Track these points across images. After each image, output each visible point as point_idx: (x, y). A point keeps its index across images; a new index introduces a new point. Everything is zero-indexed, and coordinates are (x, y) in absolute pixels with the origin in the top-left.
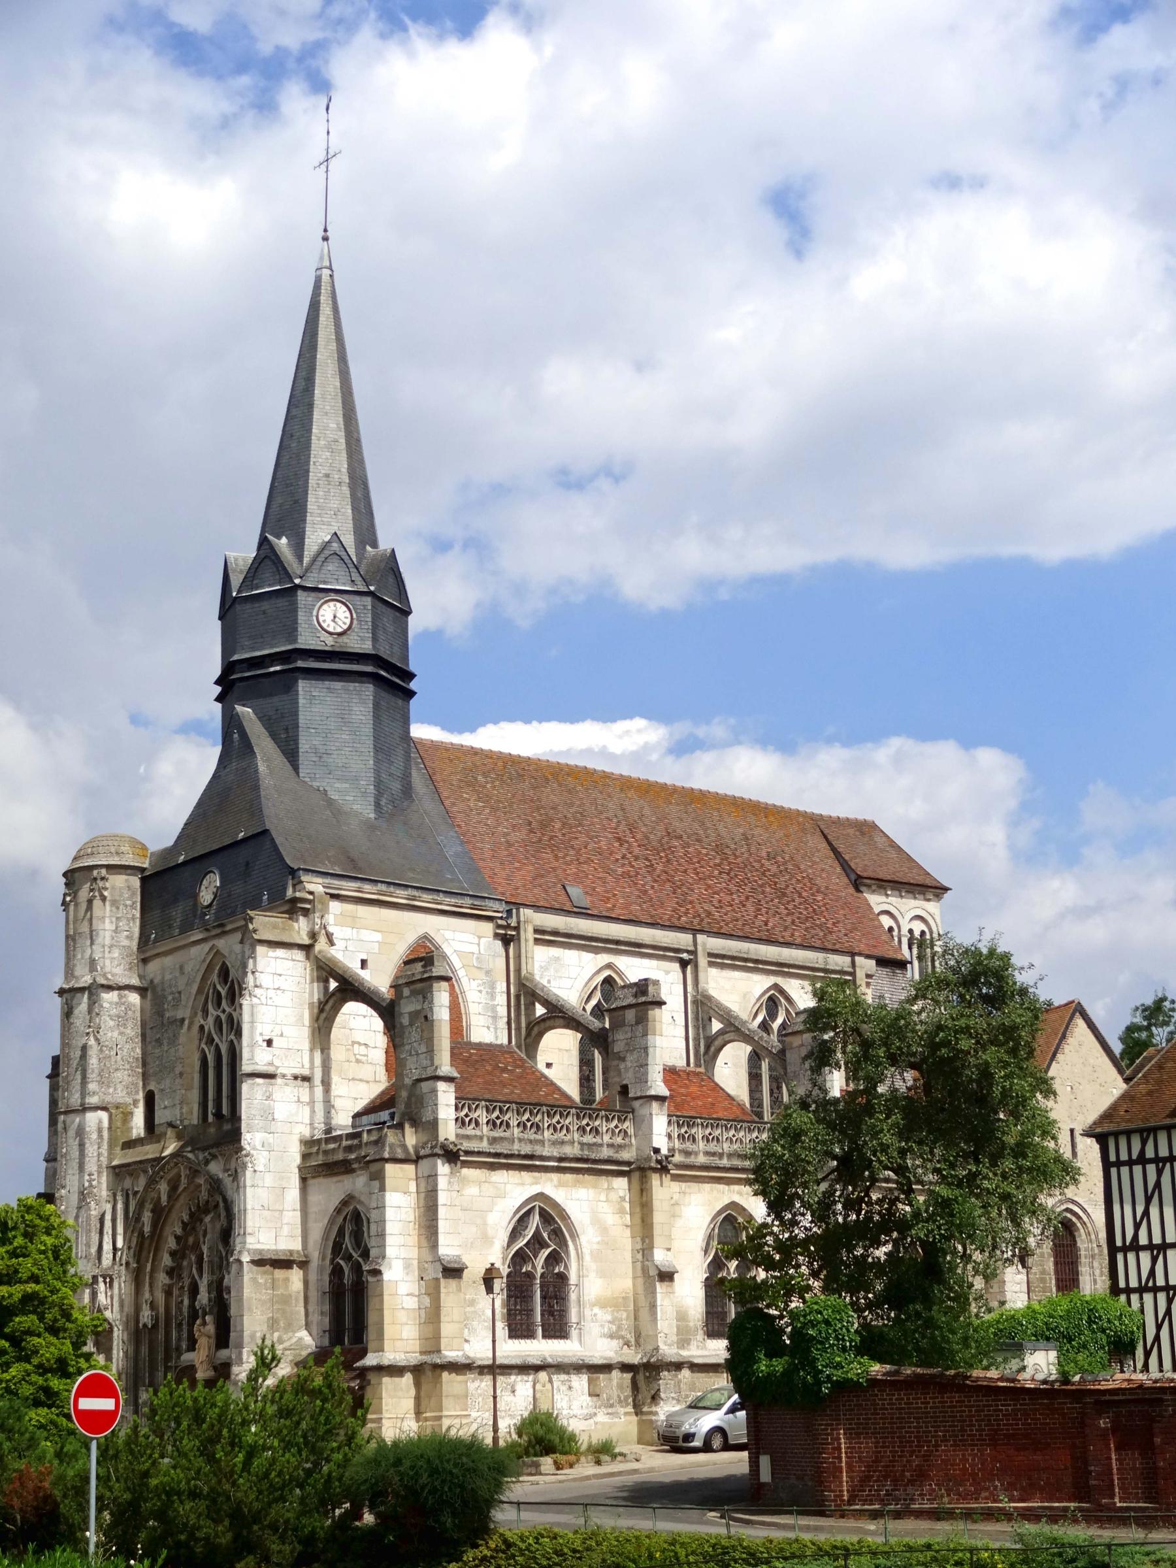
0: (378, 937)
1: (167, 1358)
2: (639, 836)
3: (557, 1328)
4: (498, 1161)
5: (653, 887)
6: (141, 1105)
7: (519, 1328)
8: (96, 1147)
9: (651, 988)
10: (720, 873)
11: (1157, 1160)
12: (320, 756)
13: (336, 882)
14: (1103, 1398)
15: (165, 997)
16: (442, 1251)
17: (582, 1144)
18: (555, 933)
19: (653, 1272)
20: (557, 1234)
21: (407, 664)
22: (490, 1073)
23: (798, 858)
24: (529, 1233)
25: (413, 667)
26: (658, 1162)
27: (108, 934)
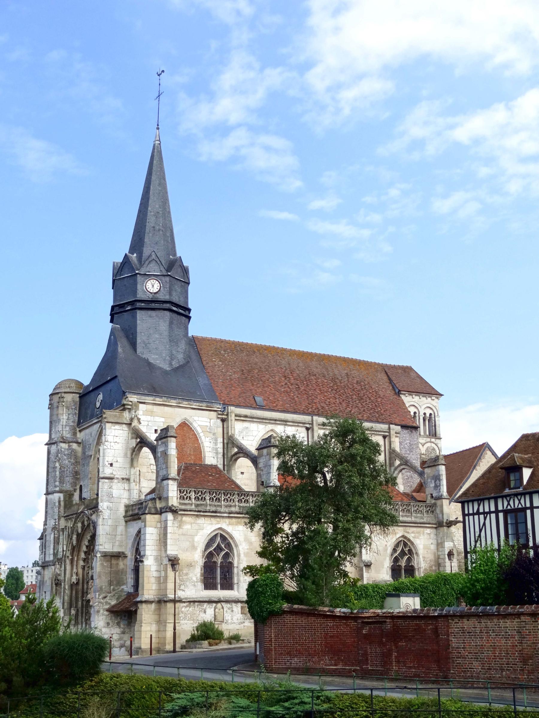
0: (163, 420)
1: (83, 596)
2: (295, 375)
3: (228, 585)
4: (200, 513)
5: (297, 397)
6: (78, 491)
7: (209, 584)
9: (272, 440)
10: (332, 390)
11: (484, 513)
12: (146, 345)
13: (143, 397)
14: (365, 620)
15: (86, 446)
16: (169, 552)
17: (239, 507)
18: (246, 416)
20: (229, 546)
21: (188, 305)
22: (204, 477)
23: (372, 383)
24: (215, 545)
25: (190, 306)
27: (64, 421)
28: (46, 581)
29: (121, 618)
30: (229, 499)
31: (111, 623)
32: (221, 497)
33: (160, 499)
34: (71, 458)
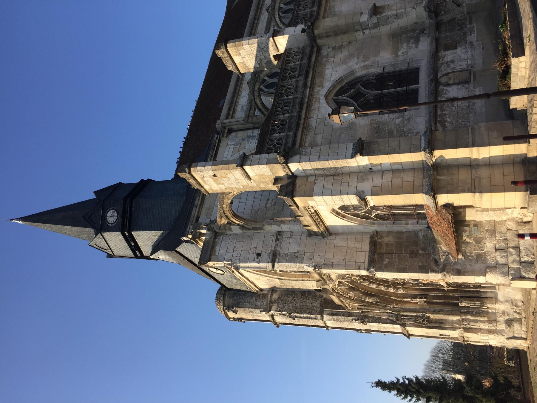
3: (410, 75)
8: (340, 317)
18: (229, 109)
19: (375, 20)
20: (352, 84)
26: (308, 27)
28: (426, 333)
30: (289, 91)
32: (283, 100)
34: (287, 301)
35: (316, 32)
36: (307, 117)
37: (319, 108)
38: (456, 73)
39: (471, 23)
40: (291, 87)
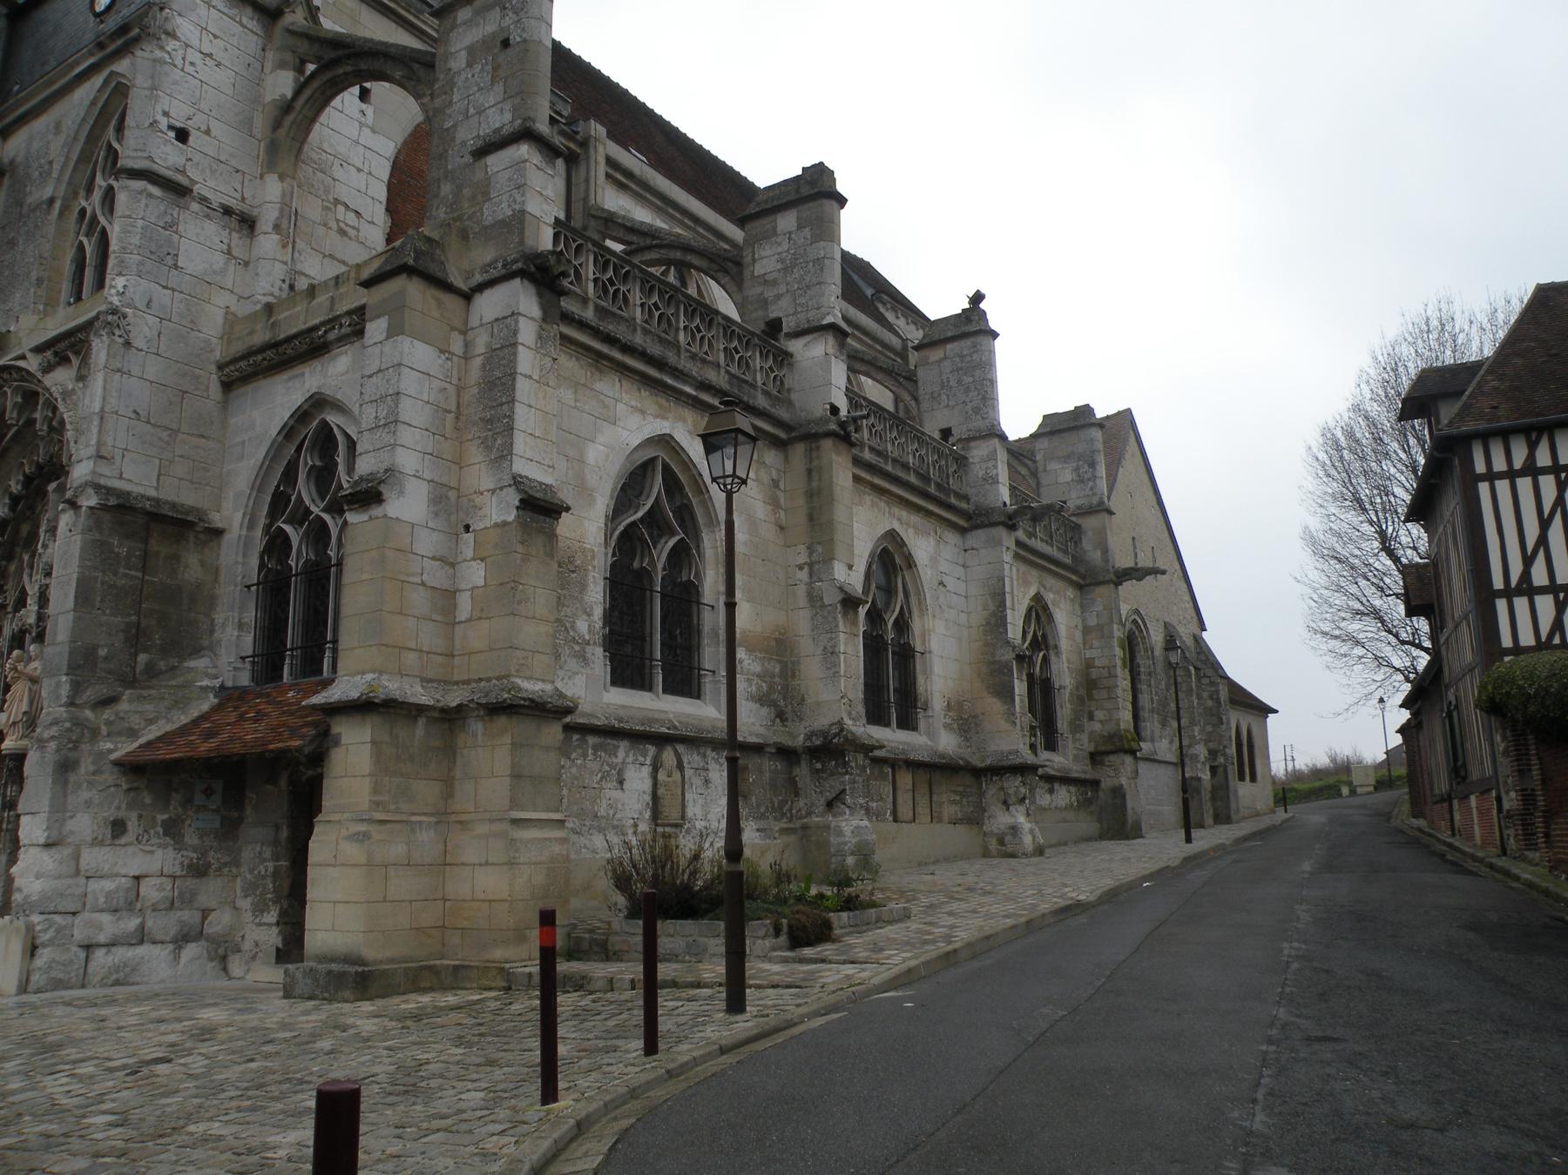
18: (629, 174)
19: (832, 598)
20: (685, 514)
29: (187, 802)
30: (698, 336)
31: (133, 825)
32: (676, 314)
33: (464, 235)
35: (827, 444)
36: (623, 370)
37: (643, 412)
38: (679, 791)
39: (783, 831)
40: (706, 348)
